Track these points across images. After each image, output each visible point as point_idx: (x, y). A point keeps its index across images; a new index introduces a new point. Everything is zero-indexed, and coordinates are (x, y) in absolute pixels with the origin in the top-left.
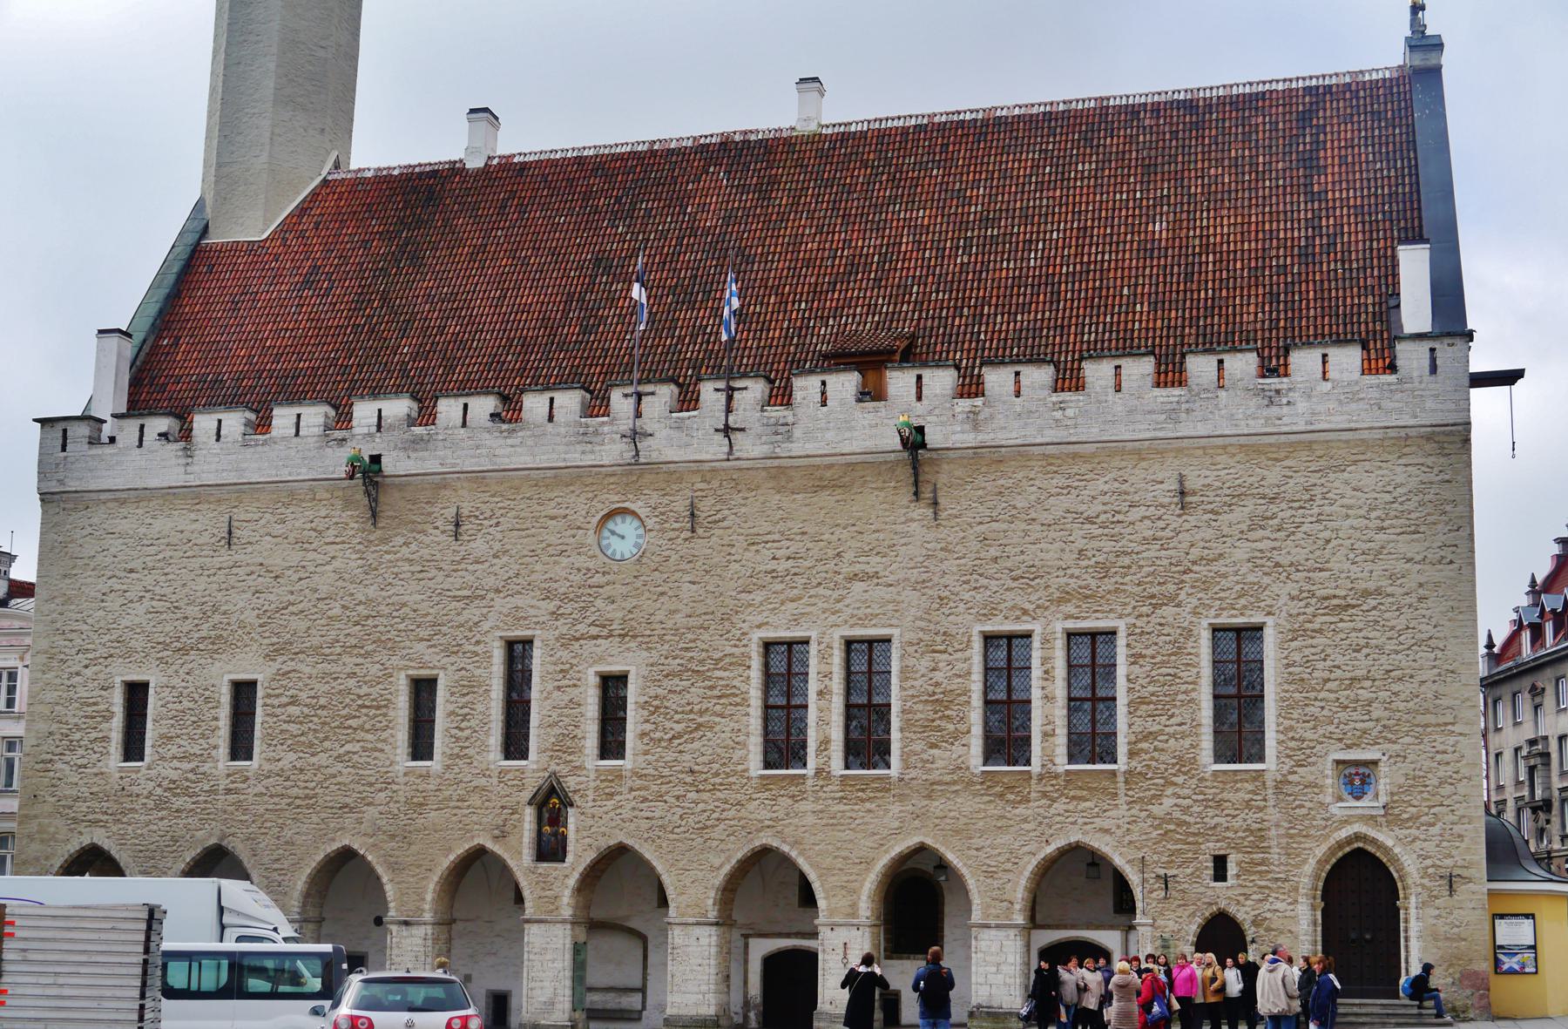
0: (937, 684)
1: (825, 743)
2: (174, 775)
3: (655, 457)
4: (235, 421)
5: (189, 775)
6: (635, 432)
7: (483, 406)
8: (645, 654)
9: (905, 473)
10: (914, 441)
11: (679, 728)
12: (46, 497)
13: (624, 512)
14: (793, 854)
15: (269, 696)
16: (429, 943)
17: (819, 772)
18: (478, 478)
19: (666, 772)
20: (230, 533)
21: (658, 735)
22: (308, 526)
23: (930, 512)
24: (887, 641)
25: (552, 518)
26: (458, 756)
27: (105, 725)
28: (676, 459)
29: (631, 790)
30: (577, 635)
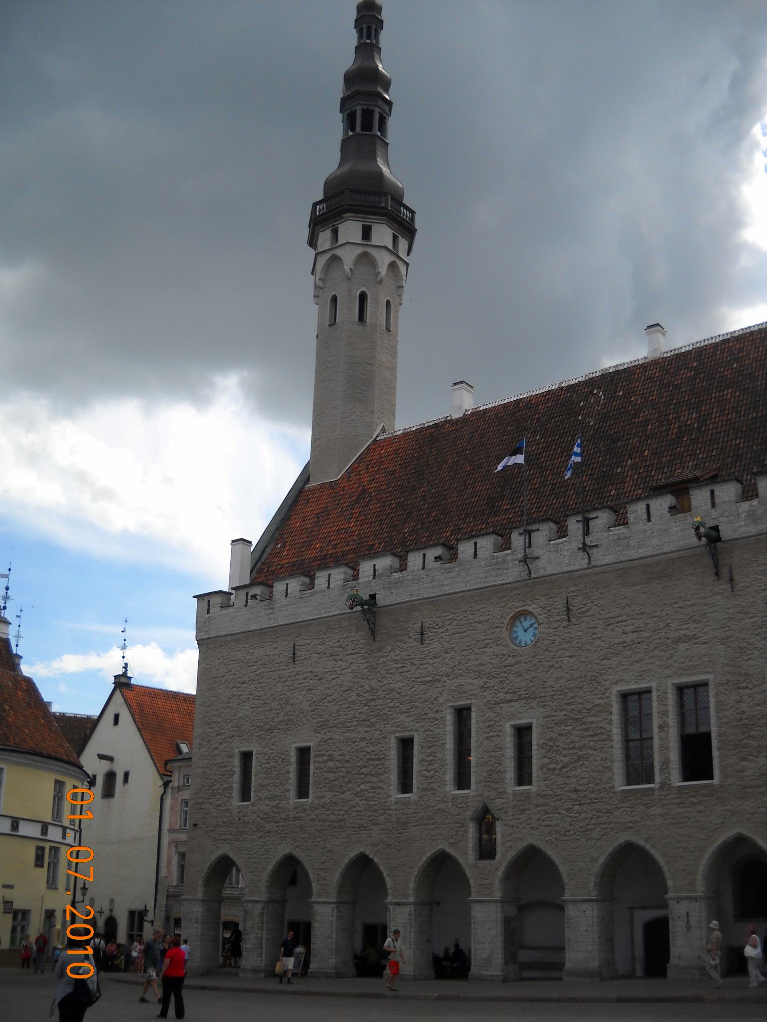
0: (743, 713)
1: (666, 763)
2: (266, 809)
3: (542, 573)
4: (295, 584)
5: (275, 809)
6: (526, 557)
7: (432, 553)
8: (542, 710)
9: (708, 561)
10: (713, 537)
11: (566, 760)
12: (201, 642)
13: (525, 614)
14: (648, 847)
15: (317, 756)
16: (413, 917)
17: (662, 785)
18: (434, 602)
19: (559, 792)
20: (294, 654)
21: (552, 766)
22: (336, 645)
23: (727, 587)
24: (705, 684)
25: (480, 622)
26: (427, 789)
27: (230, 779)
28: (554, 572)
29: (537, 806)
30: (498, 700)
